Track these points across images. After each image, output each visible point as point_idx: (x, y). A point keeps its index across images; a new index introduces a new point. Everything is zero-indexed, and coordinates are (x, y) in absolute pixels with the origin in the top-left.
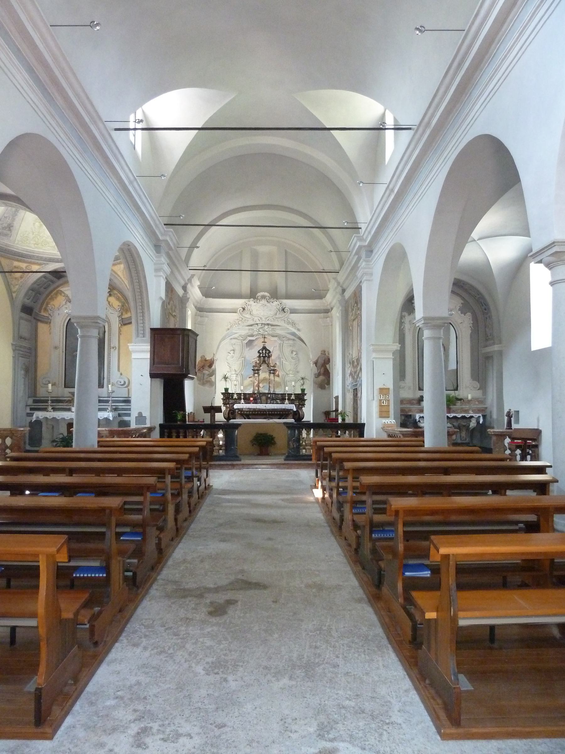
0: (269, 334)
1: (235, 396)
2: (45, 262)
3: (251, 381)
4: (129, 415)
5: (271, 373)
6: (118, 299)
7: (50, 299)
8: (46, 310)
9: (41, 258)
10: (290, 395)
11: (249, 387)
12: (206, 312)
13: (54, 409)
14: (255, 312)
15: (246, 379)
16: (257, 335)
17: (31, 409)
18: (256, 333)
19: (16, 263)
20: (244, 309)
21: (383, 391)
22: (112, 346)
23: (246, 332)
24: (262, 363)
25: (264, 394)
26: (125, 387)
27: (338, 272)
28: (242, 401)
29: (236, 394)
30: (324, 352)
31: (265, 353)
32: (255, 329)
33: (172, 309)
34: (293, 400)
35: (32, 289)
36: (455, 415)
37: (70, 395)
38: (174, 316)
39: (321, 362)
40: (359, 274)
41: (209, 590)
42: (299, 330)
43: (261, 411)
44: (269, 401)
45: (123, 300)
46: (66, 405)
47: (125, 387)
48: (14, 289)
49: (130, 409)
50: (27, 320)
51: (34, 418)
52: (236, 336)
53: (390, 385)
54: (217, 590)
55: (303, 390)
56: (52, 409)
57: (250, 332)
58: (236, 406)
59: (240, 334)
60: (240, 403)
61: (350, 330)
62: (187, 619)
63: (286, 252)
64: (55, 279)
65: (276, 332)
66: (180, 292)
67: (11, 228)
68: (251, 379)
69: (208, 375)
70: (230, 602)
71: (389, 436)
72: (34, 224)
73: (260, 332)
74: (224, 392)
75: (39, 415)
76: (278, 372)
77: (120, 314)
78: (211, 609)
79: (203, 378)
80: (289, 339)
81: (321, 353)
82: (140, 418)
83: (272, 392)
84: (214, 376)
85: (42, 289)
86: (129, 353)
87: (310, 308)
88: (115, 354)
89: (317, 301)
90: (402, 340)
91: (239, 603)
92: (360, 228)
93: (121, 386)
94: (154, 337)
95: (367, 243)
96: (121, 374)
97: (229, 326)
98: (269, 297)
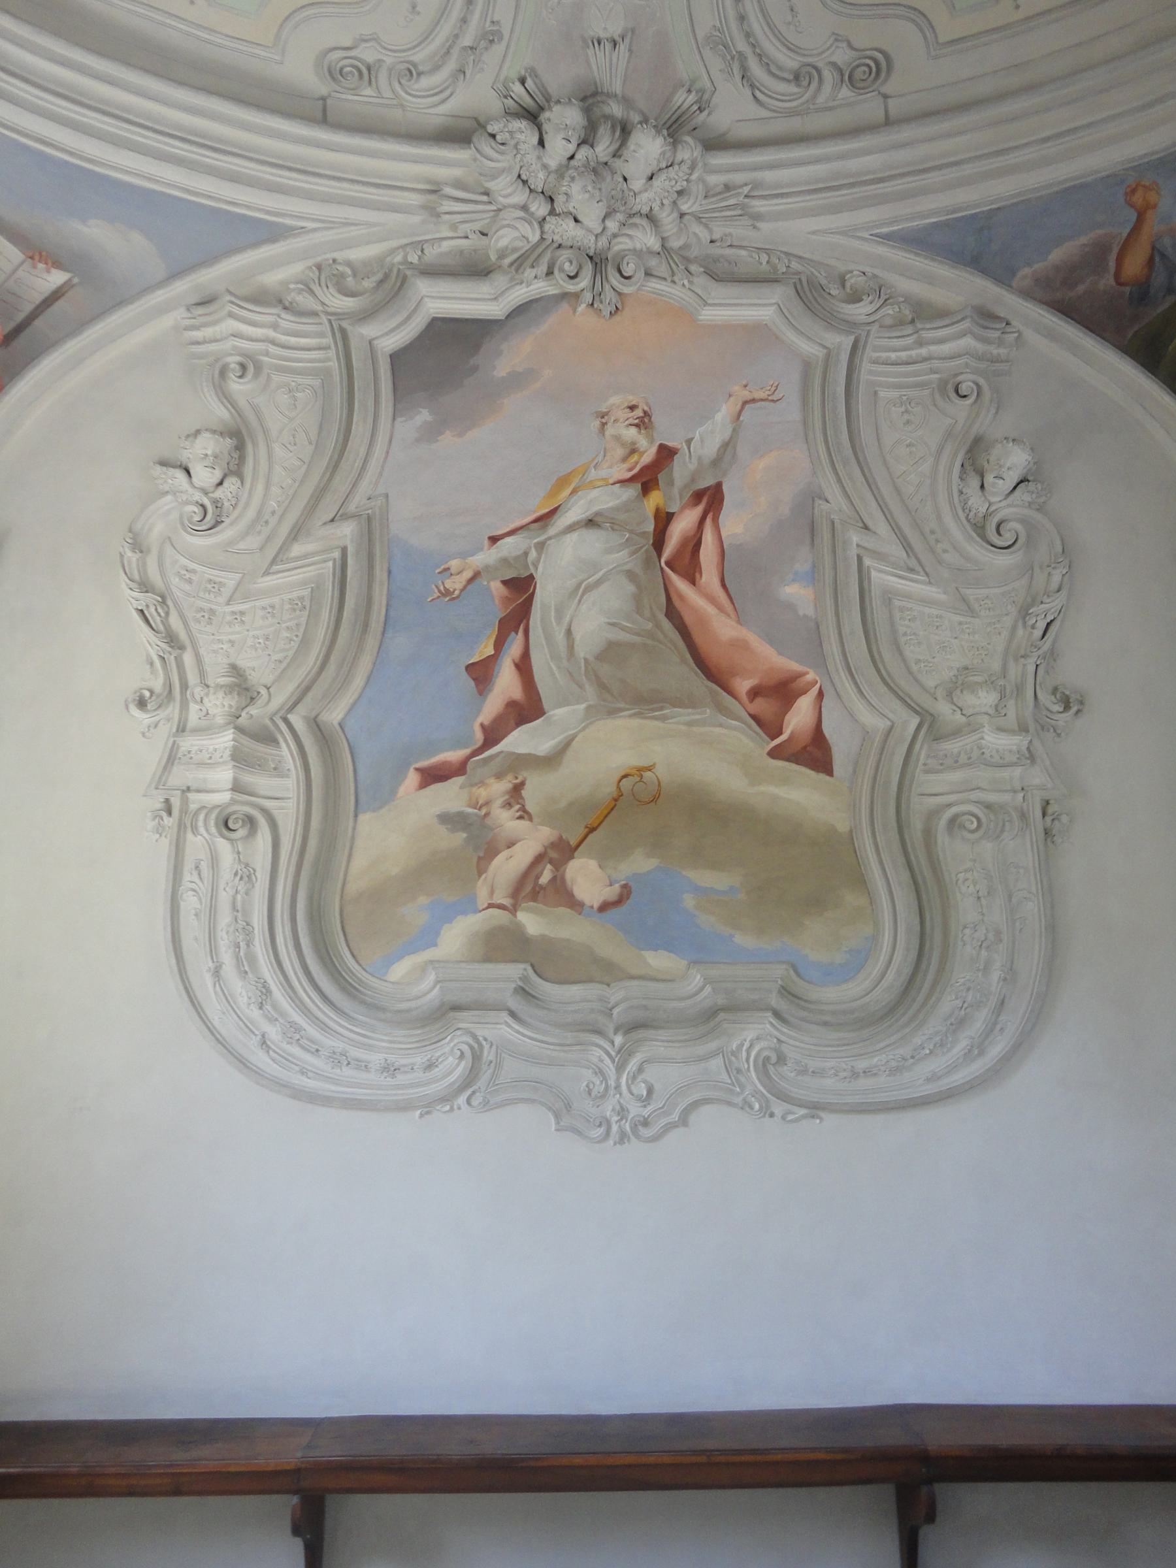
11: (416, 912)
73: (563, 230)
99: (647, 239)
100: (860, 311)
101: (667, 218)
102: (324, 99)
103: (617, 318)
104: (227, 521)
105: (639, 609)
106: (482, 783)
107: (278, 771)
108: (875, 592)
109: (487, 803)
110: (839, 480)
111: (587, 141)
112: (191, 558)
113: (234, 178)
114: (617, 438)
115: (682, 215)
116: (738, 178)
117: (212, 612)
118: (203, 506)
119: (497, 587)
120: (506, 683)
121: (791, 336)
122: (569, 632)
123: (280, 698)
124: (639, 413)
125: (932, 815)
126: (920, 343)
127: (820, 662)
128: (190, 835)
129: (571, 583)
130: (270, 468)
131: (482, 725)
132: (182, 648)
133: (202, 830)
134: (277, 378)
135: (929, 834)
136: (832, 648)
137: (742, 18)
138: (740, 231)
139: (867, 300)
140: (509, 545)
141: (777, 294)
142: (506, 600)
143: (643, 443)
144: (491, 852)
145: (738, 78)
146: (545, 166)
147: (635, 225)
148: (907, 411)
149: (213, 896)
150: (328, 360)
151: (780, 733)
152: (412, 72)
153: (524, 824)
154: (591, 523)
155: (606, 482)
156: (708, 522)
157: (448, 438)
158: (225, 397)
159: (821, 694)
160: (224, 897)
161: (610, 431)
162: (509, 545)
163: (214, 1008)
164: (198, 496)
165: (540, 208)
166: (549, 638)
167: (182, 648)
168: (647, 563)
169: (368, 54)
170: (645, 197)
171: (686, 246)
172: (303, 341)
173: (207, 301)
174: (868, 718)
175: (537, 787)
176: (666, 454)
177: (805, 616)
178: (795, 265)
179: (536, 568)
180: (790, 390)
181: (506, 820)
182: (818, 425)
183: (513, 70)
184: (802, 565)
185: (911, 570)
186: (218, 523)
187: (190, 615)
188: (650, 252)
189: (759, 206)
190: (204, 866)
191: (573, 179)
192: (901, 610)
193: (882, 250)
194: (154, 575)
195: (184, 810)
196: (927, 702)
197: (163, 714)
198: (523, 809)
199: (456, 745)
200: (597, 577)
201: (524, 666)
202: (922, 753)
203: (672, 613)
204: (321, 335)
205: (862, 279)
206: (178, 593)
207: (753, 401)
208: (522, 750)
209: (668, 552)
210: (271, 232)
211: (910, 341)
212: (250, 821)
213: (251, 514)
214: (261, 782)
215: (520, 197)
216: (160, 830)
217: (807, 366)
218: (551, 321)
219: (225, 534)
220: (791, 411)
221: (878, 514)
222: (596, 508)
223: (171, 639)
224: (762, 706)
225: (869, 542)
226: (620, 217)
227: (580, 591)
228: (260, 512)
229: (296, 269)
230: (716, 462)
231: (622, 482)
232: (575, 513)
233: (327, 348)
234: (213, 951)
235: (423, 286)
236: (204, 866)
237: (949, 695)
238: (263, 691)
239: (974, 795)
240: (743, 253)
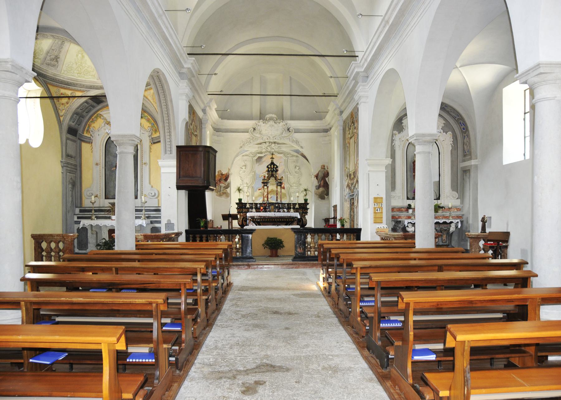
1: (248, 206)
2: (86, 89)
3: (261, 193)
4: (159, 222)
5: (278, 185)
6: (148, 120)
7: (92, 122)
8: (88, 131)
9: (83, 86)
10: (294, 204)
11: (259, 198)
12: (222, 132)
13: (98, 218)
14: (264, 132)
15: (256, 191)
16: (265, 152)
17: (78, 218)
18: (264, 150)
19: (63, 91)
20: (254, 129)
21: (377, 200)
22: (144, 162)
23: (257, 149)
24: (271, 177)
25: (272, 204)
26: (156, 198)
27: (337, 96)
28: (254, 210)
29: (249, 204)
30: (323, 167)
31: (274, 167)
32: (263, 147)
33: (194, 129)
34: (297, 208)
35: (76, 113)
36: (445, 221)
37: (110, 205)
38: (196, 136)
39: (321, 175)
40: (356, 97)
41: (239, 372)
42: (302, 147)
43: (270, 219)
45: (153, 122)
46: (107, 214)
47: (156, 198)
48: (61, 114)
49: (160, 217)
50: (72, 140)
51: (81, 226)
53: (383, 195)
54: (247, 372)
55: (306, 200)
56: (96, 217)
57: (259, 150)
58: (248, 214)
60: (252, 212)
61: (347, 147)
62: (224, 397)
63: (291, 78)
64: (95, 104)
66: (200, 114)
67: (58, 59)
68: (260, 191)
69: (224, 187)
70: (258, 383)
71: (382, 239)
72: (77, 55)
73: (268, 150)
74: (238, 202)
75: (85, 223)
77: (150, 134)
78: (244, 389)
80: (293, 156)
82: (169, 225)
83: (279, 202)
85: (84, 114)
86: (158, 168)
87: (313, 128)
88: (146, 169)
89: (318, 122)
90: (393, 156)
91: (267, 383)
92: (358, 56)
93: (152, 197)
94: (180, 153)
95: (363, 70)
96: (152, 187)
97: (242, 145)
98: (276, 118)
100: (288, 155)
101: (275, 149)
140: (264, 174)
162: (264, 174)
173: (243, 156)
180: (283, 162)
210: (248, 151)
214: (248, 190)
218: (267, 156)
220: (283, 163)
235: (258, 154)
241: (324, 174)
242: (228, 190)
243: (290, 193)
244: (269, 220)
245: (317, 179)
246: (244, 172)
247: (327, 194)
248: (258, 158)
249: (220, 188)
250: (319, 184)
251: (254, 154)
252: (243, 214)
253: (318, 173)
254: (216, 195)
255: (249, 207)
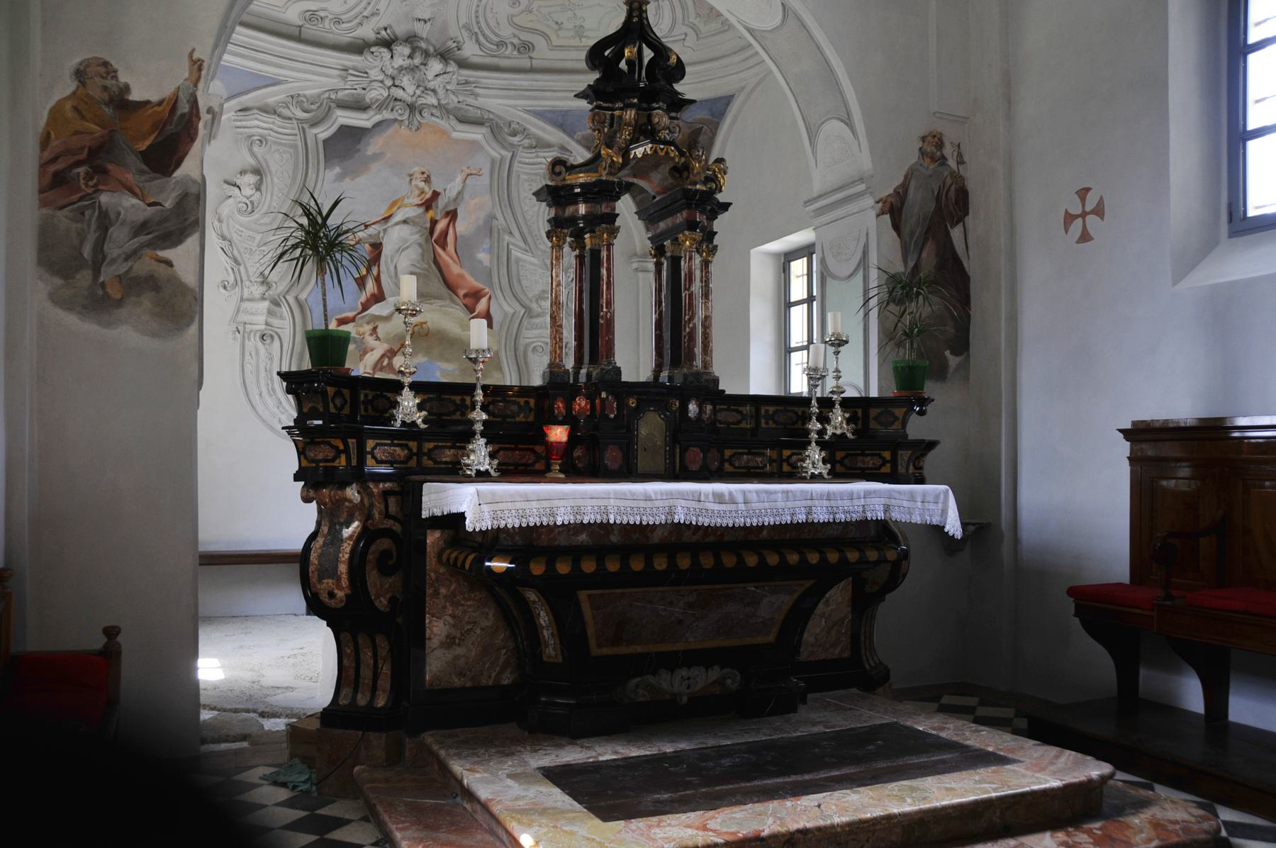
0: (444, 110)
1: (408, 407)
16: (382, 106)
18: (377, 93)
23: (335, 82)
28: (479, 455)
30: (933, 146)
32: (375, 74)
39: (919, 202)
44: (695, 457)
52: (272, 96)
59: (292, 87)
65: (481, 101)
69: (143, 227)
73: (398, 93)
76: (484, 301)
79: (99, 248)
81: (922, 152)
84: (191, 242)
99: (431, 100)
100: (515, 140)
101: (441, 92)
102: (300, 27)
103: (418, 132)
104: (256, 211)
105: (423, 260)
106: (361, 326)
107: (282, 318)
108: (513, 258)
109: (363, 334)
110: (502, 213)
111: (411, 57)
112: (240, 226)
113: (263, 62)
114: (417, 186)
115: (447, 90)
116: (471, 79)
117: (251, 249)
118: (246, 204)
119: (367, 246)
120: (370, 286)
121: (488, 148)
122: (396, 267)
123: (282, 287)
124: (425, 176)
125: (527, 345)
126: (537, 157)
127: (491, 285)
128: (247, 341)
129: (397, 247)
130: (273, 188)
131: (361, 303)
132: (240, 264)
133: (252, 340)
134: (274, 147)
135: (525, 353)
136: (495, 280)
137: (478, 23)
138: (470, 100)
139: (518, 136)
141: (484, 130)
142: (371, 252)
143: (427, 189)
144: (365, 352)
145: (474, 41)
146: (393, 67)
147: (427, 94)
148: (530, 185)
149: (258, 366)
150: (295, 140)
151: (474, 312)
152: (338, 21)
153: (378, 342)
154: (405, 222)
155: (411, 205)
156: (451, 225)
157: (347, 180)
158: (253, 155)
159: (490, 297)
160: (262, 366)
161: (413, 182)
162: (371, 230)
163: (260, 408)
164: (245, 200)
165: (389, 82)
166: (388, 269)
167: (240, 264)
168: (427, 240)
169: (322, 14)
170: (433, 83)
171: (448, 104)
172: (285, 131)
174: (507, 308)
175: (382, 329)
176: (436, 195)
177: (486, 267)
178: (491, 116)
179: (383, 238)
180: (486, 171)
181: (370, 341)
182: (496, 189)
183: (382, 24)
184: (486, 246)
185: (527, 251)
186: (253, 211)
187: (242, 250)
188: (433, 106)
189: (478, 91)
190: (253, 353)
191: (404, 75)
192: (522, 266)
193: (526, 116)
194: (226, 233)
195: (244, 332)
196: (528, 302)
197: (233, 292)
198: (377, 337)
199: (351, 310)
200: (407, 244)
201: (378, 280)
202: (525, 323)
203: (436, 262)
204: (294, 129)
205: (517, 126)
206: (236, 241)
207: (471, 174)
208: (377, 314)
209: (435, 236)
210: (276, 83)
211: (534, 155)
212: (272, 337)
213: (265, 208)
214: (275, 322)
215: (381, 77)
216: (235, 339)
217: (493, 161)
218: (391, 131)
219: (255, 216)
220: (485, 180)
221: (516, 229)
222: (407, 216)
223: (236, 261)
224: (467, 301)
225: (512, 240)
226: (421, 88)
227: (400, 250)
228: (269, 207)
229: (282, 97)
230: (455, 200)
231: (418, 205)
232: (399, 217)
233: (296, 135)
234: (258, 387)
235: (339, 112)
236: (253, 353)
237: (537, 301)
238: (274, 284)
239: (543, 340)
240: (471, 108)
241: (938, 198)
242: (180, 256)
243: (521, 349)
244: (684, 562)
245: (896, 227)
246: (251, 208)
247: (961, 344)
248: (335, 133)
249: (92, 237)
250: (911, 264)
251: (320, 110)
252: (364, 490)
253: (905, 186)
254: (55, 299)
255: (419, 418)
